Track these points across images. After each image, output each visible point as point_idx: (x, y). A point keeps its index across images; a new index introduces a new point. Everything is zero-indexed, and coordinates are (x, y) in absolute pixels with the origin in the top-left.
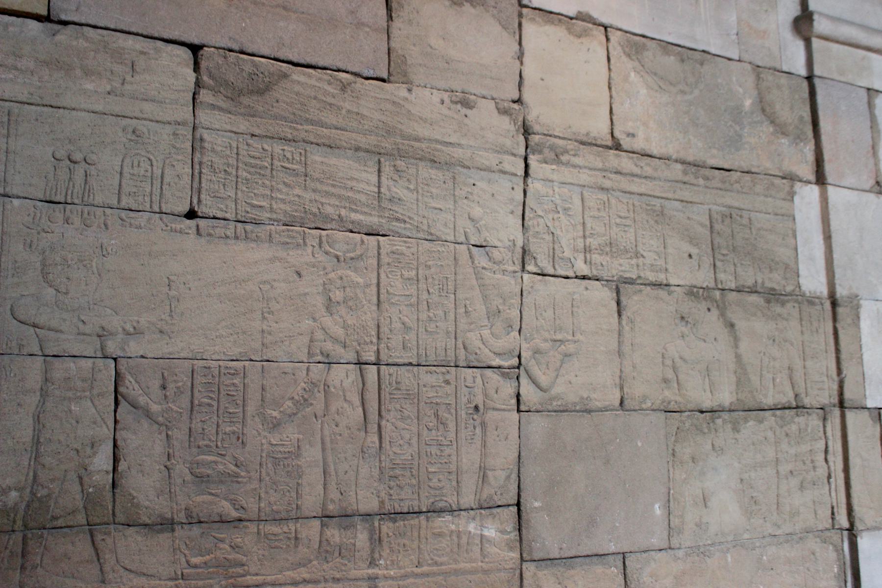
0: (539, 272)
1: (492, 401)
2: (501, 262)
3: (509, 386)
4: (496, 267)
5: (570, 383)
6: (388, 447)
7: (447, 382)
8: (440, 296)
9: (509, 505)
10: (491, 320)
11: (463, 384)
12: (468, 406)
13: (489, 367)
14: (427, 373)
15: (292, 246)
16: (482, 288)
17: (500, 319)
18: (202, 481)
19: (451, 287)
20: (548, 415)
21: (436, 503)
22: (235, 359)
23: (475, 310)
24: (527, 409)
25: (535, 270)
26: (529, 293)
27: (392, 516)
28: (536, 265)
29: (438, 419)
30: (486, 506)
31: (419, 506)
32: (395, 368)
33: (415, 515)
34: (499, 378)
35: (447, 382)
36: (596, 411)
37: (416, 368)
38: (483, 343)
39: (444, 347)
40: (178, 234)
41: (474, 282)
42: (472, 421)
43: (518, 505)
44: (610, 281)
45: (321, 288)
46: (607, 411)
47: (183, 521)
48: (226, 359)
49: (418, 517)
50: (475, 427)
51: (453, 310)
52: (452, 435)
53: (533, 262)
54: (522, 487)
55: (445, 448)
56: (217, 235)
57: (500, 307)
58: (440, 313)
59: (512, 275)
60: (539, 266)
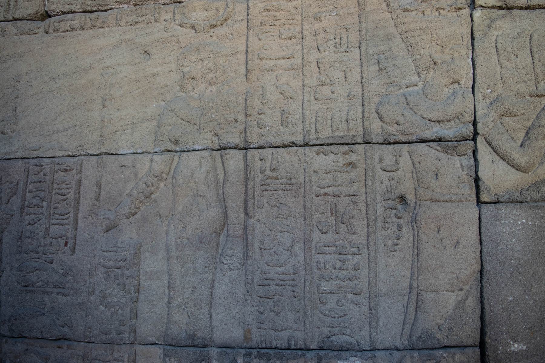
6: (257, 256)
9: (465, 347)
10: (423, 76)
11: (378, 167)
13: (423, 141)
14: (318, 154)
15: (141, 25)
16: (404, 36)
18: (27, 292)
19: (353, 38)
21: (334, 338)
22: (71, 154)
24: (493, 199)
27: (263, 351)
29: (337, 217)
30: (421, 347)
31: (305, 340)
32: (270, 151)
33: (299, 353)
34: (441, 155)
37: (301, 149)
39: (344, 117)
40: (28, 36)
42: (395, 219)
43: (482, 345)
45: (173, 66)
47: (6, 334)
48: (61, 155)
49: (303, 355)
50: (400, 228)
51: (359, 69)
52: (360, 238)
54: (487, 319)
55: (349, 257)
56: (63, 29)
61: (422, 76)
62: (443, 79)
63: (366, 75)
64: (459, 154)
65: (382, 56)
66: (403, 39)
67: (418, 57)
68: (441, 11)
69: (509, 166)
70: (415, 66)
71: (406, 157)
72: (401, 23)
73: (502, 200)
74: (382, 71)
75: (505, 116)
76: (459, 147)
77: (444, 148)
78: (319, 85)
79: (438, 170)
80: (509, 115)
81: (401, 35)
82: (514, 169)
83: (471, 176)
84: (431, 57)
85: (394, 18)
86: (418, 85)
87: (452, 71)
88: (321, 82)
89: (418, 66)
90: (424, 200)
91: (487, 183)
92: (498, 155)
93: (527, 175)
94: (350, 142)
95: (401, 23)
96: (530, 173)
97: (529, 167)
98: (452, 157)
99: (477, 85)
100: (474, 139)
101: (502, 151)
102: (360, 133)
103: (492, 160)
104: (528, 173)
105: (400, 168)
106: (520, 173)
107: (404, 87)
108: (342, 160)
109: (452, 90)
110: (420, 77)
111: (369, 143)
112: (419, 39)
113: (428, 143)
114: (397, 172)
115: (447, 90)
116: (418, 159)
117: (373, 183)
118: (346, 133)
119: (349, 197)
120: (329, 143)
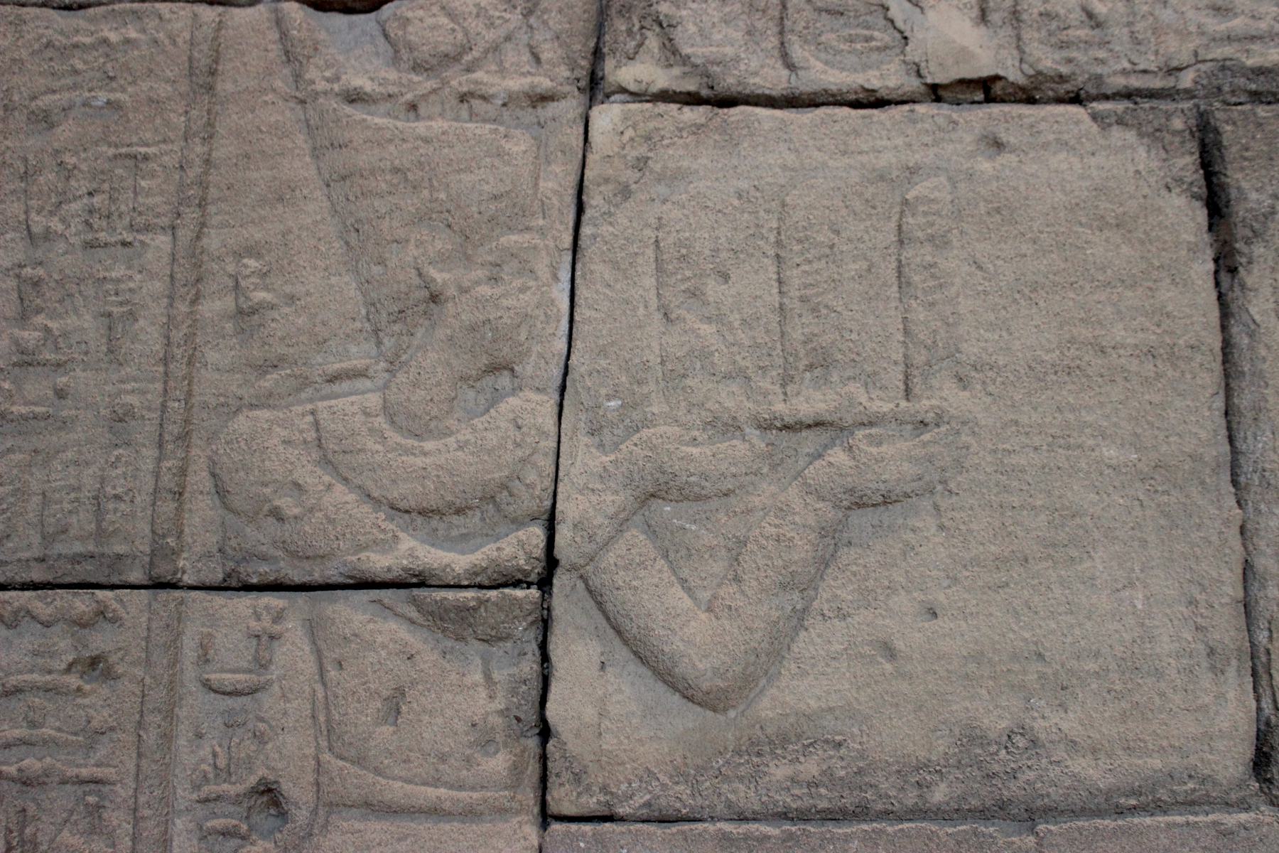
0: (690, 86)
1: (360, 761)
2: (450, 59)
3: (478, 677)
4: (425, 84)
5: (889, 651)
7: (94, 665)
8: (90, 245)
10: (388, 342)
11: (190, 673)
12: (209, 790)
17: (441, 333)
20: (725, 837)
23: (292, 299)
24: (591, 803)
25: (662, 79)
26: (625, 192)
28: (671, 53)
35: (94, 665)
36: (1075, 813)
38: (326, 462)
41: (300, 167)
44: (1152, 94)
46: (1159, 807)
53: (653, 43)
57: (439, 276)
58: (85, 323)
59: (528, 116)
60: (685, 60)
61: (386, 341)
62: (457, 355)
63: (181, 334)
64: (484, 637)
65: (252, 263)
66: (335, 201)
67: (376, 270)
68: (476, 103)
69: (660, 684)
70: (365, 303)
71: (298, 641)
72: (332, 145)
73: (621, 810)
74: (247, 318)
75: (663, 499)
76: (482, 610)
77: (431, 613)
78: (14, 365)
79: (403, 694)
80: (675, 494)
81: (328, 186)
82: (677, 696)
83: (518, 719)
84: (420, 275)
85: (312, 122)
86: (371, 372)
87: (488, 326)
88: (22, 353)
89: (373, 304)
90: (344, 805)
91: (573, 746)
92: (626, 642)
93: (721, 718)
94: (103, 580)
95: (332, 145)
96: (732, 714)
97: (725, 691)
98: (458, 645)
99: (574, 381)
100: (545, 583)
101: (635, 631)
102: (141, 548)
103: (603, 659)
104: (725, 710)
105: (269, 683)
106: (699, 709)
107: (319, 379)
108: (64, 646)
109: (488, 396)
110: (379, 343)
111: (174, 586)
112: (380, 205)
113: (378, 591)
114: (258, 695)
115: (471, 394)
116: (337, 651)
117: (167, 738)
118: (91, 548)
119: (76, 787)
120: (29, 580)
